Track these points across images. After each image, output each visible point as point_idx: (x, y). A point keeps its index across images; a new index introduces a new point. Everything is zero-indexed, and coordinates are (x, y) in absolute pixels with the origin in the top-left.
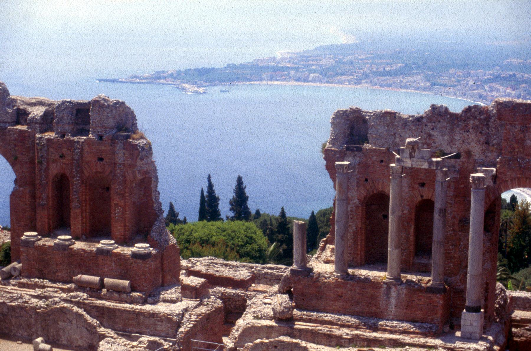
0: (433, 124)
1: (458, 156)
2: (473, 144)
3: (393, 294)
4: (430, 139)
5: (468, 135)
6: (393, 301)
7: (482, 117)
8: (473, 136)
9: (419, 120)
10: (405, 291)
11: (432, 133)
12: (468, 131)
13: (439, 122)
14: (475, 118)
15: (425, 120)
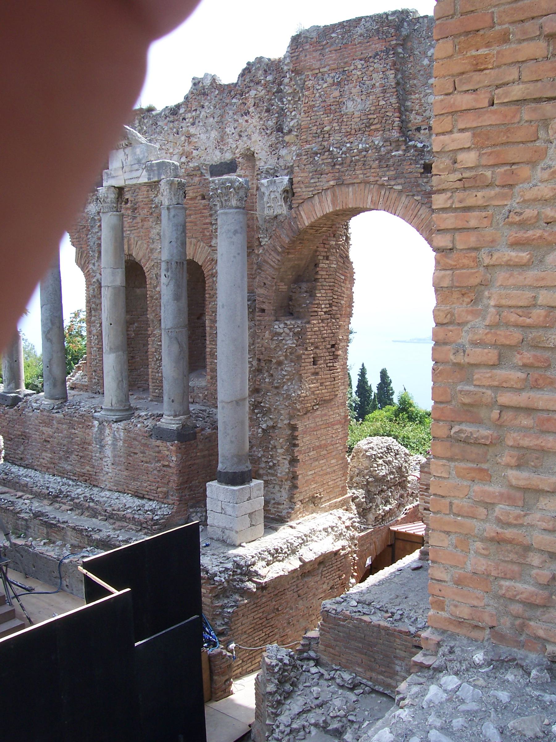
0: (194, 113)
1: (230, 167)
2: (256, 137)
3: (109, 440)
4: (189, 143)
5: (247, 121)
6: (108, 452)
7: (269, 78)
8: (254, 121)
9: (174, 111)
10: (122, 434)
11: (192, 130)
12: (247, 113)
13: (203, 107)
14: (258, 83)
15: (182, 111)
